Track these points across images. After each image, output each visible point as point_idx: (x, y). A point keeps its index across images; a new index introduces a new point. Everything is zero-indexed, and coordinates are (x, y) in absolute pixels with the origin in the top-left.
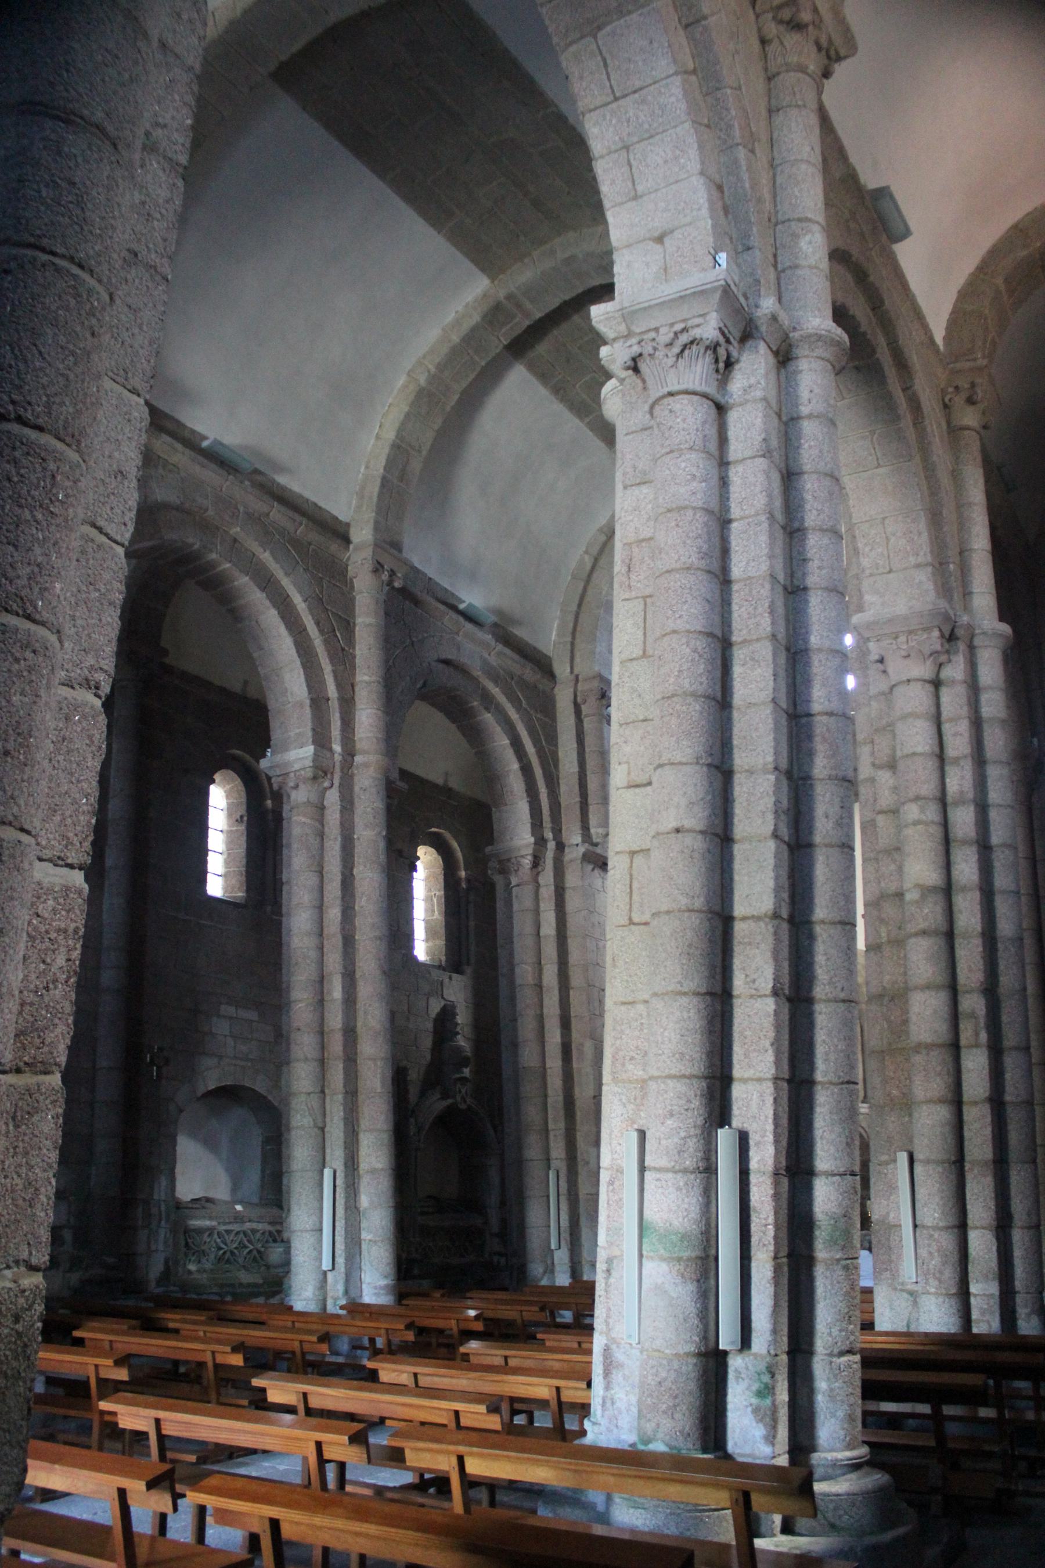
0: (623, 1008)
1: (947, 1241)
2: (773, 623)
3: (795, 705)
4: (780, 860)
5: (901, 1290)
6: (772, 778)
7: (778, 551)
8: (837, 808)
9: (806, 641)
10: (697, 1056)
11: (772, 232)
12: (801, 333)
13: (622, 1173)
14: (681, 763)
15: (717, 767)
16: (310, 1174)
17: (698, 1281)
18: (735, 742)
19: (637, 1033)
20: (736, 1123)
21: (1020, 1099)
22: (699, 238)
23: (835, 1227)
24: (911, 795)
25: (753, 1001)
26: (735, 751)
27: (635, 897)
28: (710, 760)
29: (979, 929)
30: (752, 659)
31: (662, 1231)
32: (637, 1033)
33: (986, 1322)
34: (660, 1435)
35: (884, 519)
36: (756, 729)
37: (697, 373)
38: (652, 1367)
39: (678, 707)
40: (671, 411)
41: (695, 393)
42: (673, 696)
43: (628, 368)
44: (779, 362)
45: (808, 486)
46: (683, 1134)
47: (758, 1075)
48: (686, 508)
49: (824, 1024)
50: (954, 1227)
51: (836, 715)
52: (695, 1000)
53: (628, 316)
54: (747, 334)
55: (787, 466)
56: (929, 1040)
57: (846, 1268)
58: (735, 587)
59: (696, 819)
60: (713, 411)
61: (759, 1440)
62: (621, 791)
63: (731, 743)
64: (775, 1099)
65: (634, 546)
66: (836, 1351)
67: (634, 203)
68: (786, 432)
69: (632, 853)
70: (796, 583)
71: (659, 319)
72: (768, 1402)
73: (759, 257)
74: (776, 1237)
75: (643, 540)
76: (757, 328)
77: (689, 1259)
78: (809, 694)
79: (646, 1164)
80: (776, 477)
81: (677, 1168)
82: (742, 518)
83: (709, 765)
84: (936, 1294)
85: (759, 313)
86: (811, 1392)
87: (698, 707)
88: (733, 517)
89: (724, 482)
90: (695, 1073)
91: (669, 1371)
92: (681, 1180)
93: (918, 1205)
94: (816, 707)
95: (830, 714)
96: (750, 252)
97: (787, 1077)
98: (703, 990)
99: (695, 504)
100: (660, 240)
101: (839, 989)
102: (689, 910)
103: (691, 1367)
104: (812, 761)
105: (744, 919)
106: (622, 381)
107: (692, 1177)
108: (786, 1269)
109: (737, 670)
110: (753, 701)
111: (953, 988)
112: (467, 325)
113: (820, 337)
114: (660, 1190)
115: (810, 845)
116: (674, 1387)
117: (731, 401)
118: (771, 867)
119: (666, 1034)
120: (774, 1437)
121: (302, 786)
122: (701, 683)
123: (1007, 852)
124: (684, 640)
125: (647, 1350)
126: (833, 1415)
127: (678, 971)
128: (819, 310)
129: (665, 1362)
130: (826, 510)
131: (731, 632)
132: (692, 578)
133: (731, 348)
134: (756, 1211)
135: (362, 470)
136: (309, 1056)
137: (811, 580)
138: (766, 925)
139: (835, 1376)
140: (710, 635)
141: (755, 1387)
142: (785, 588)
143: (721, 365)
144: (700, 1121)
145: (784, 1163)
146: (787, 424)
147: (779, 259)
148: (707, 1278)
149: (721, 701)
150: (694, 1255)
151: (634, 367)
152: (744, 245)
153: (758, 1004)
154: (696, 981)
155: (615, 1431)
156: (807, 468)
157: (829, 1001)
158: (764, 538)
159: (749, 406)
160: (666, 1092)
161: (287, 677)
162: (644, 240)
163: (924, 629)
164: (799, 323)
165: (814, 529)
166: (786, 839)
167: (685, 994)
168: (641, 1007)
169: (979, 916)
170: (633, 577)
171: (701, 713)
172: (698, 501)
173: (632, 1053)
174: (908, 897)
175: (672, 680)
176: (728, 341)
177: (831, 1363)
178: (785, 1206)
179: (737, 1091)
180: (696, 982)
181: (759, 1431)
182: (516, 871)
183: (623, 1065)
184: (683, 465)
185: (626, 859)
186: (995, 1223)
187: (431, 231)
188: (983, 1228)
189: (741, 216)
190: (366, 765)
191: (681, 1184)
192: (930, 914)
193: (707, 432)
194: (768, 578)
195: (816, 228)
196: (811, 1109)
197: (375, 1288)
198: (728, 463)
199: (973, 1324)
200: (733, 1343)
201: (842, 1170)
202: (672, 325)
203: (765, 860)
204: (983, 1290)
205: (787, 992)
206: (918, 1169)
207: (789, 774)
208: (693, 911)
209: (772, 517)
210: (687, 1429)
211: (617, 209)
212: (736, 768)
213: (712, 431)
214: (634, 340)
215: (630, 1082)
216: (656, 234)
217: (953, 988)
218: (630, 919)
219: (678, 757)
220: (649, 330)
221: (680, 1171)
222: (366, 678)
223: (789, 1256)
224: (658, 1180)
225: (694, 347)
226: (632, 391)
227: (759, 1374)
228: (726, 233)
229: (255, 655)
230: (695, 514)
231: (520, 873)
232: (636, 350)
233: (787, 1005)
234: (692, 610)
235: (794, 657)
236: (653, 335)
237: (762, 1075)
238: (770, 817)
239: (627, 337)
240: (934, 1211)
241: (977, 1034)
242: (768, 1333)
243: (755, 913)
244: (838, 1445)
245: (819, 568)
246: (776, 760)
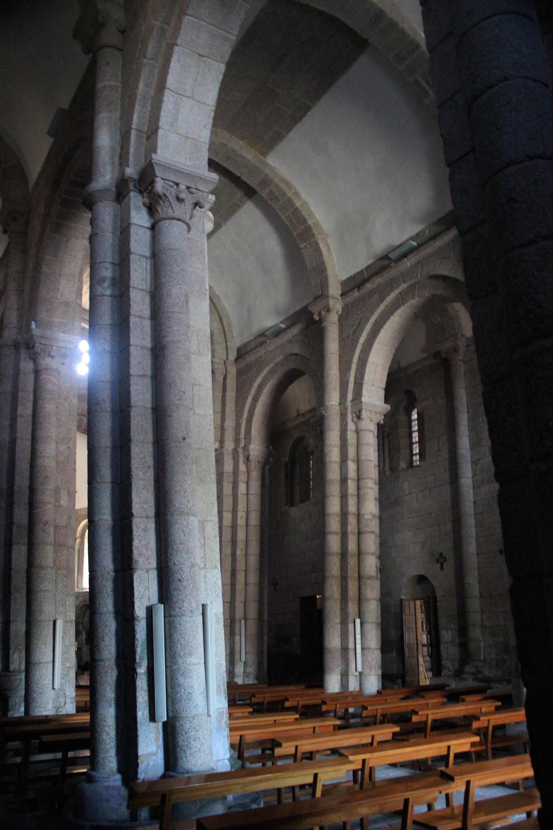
35: (377, 365)
84: (374, 675)
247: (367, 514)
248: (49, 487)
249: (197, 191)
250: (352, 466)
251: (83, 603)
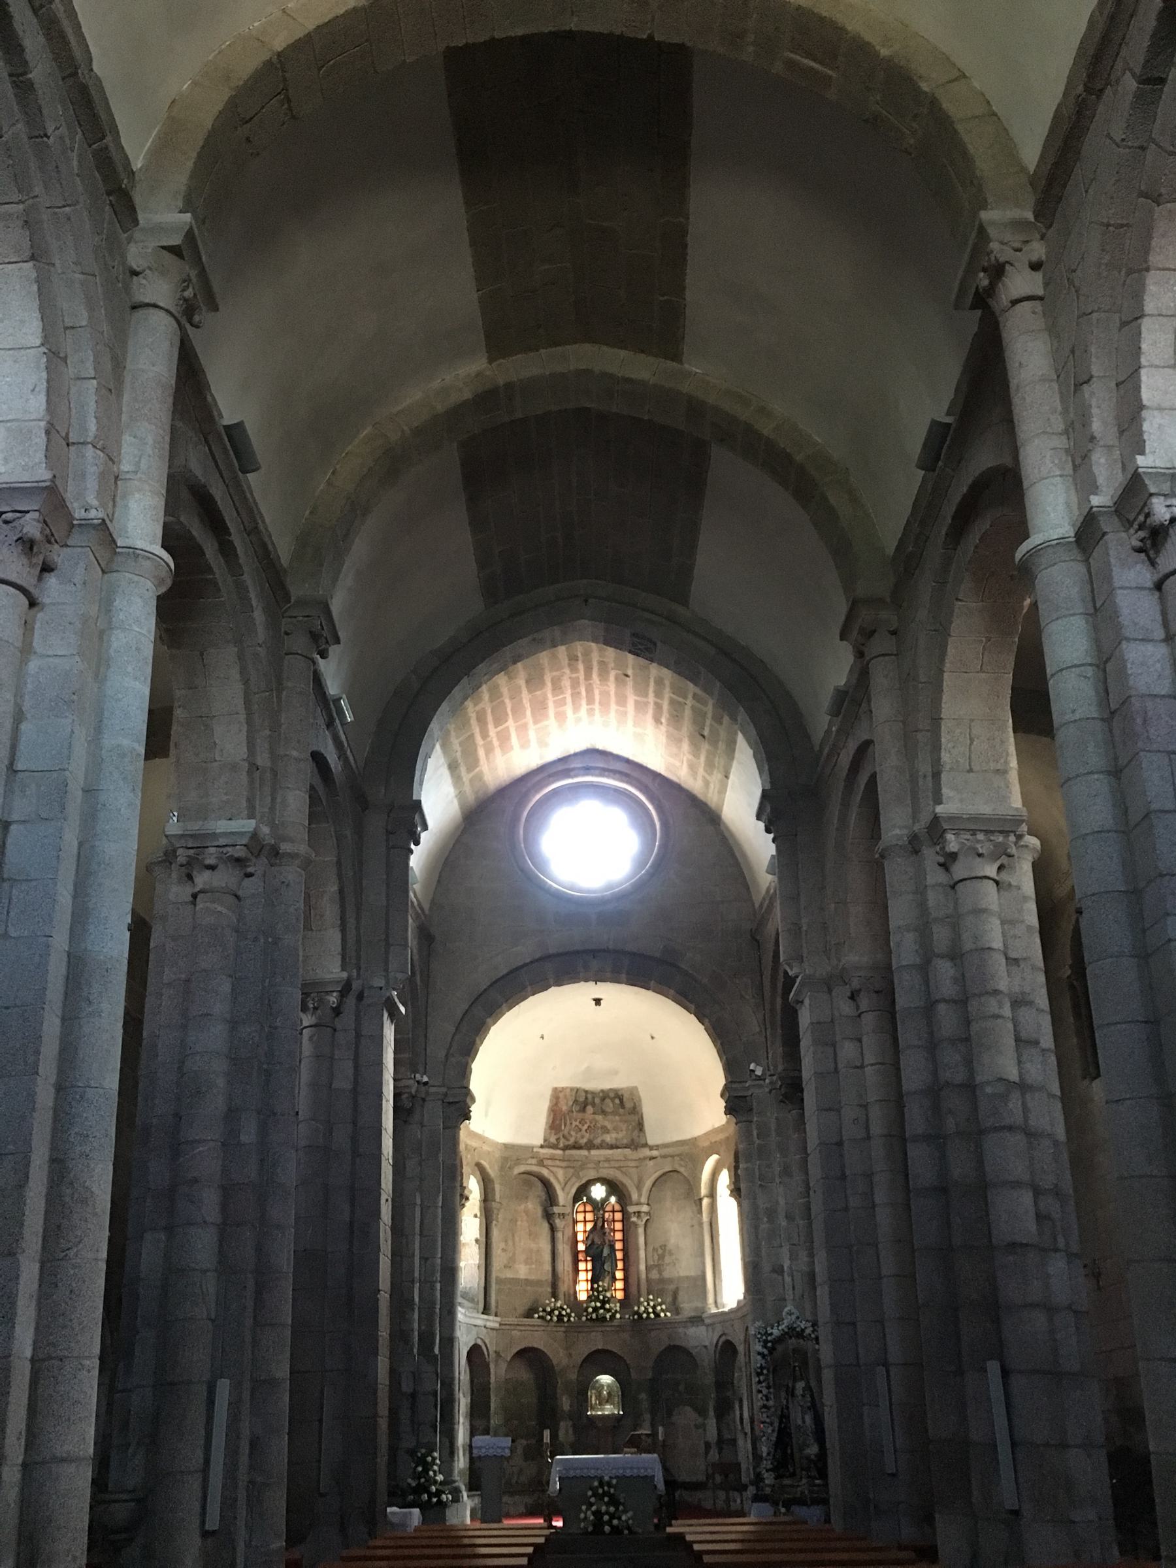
112: (454, 399)
121: (221, 866)
135: (307, 512)
136: (209, 1219)
222: (295, 753)
247: (988, 1083)
249: (18, 515)
250: (944, 970)
251: (723, 1339)
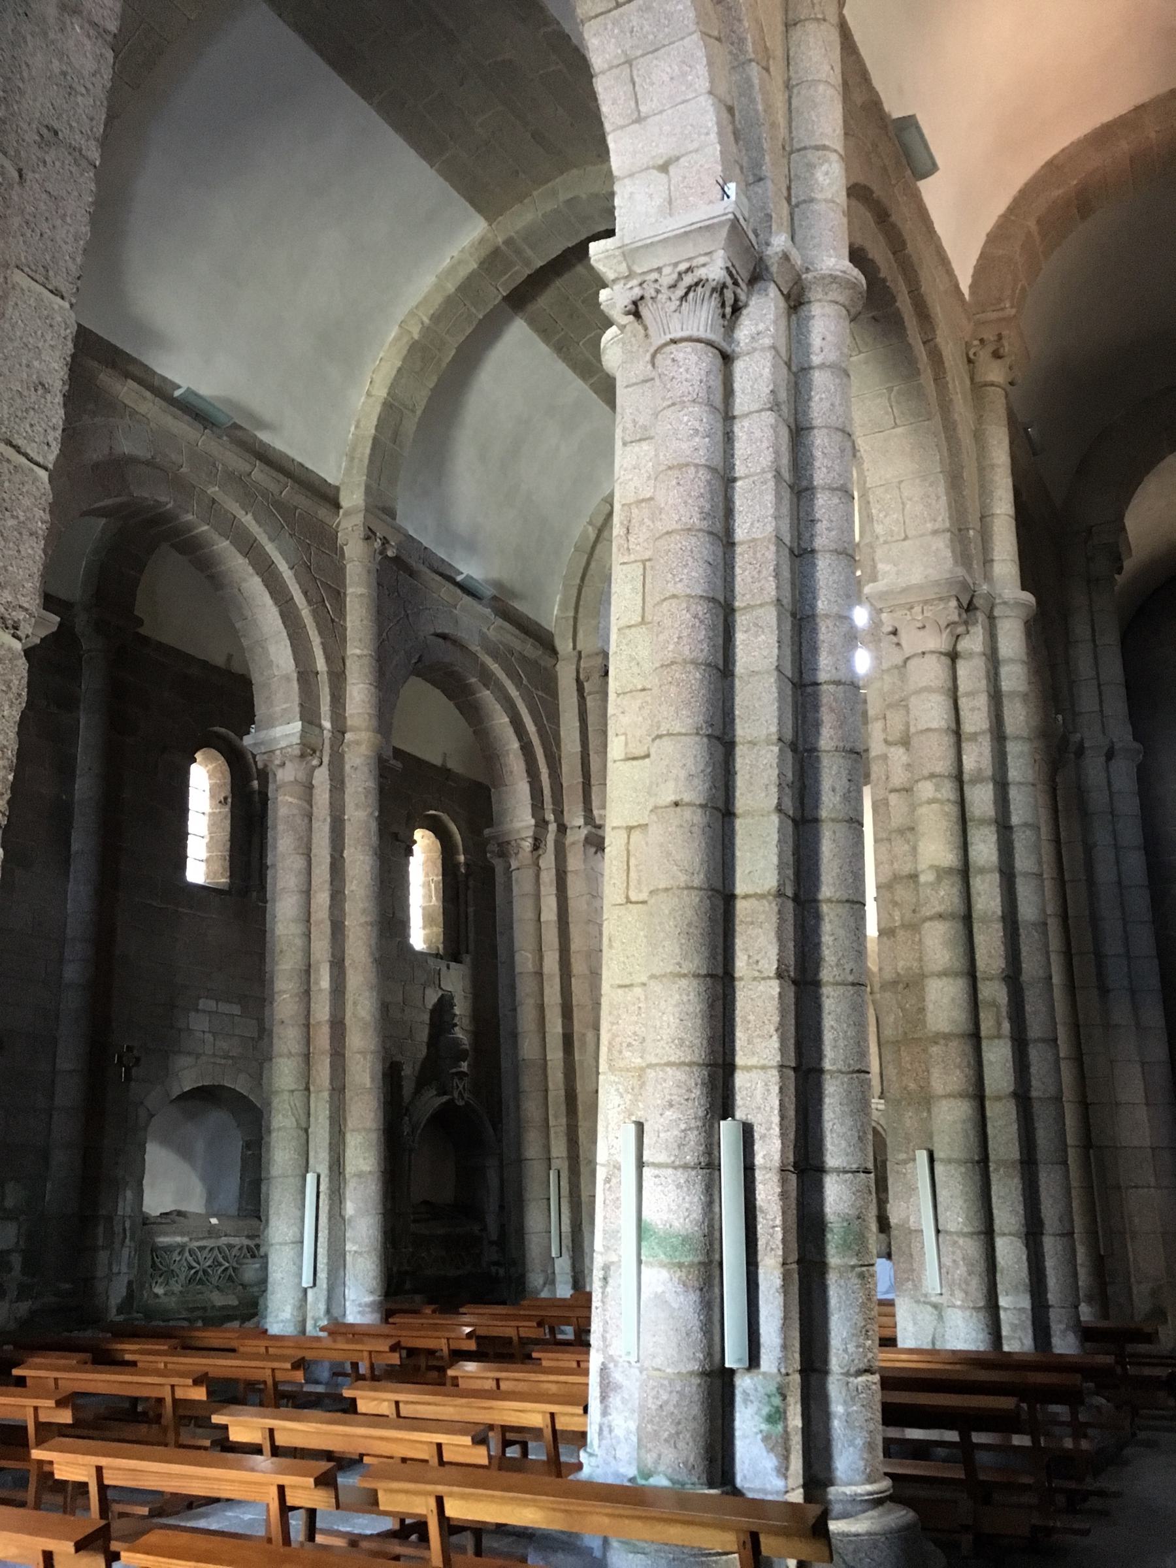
0: (620, 991)
1: (972, 1248)
2: (777, 588)
3: (801, 673)
4: (784, 835)
5: (925, 1303)
6: (776, 749)
7: (785, 510)
8: (845, 780)
9: (813, 607)
10: (697, 1041)
11: (785, 161)
12: (815, 274)
13: (619, 1169)
14: (680, 734)
15: (718, 738)
16: (291, 1180)
17: (701, 1290)
18: (737, 713)
19: (635, 1018)
20: (739, 1114)
21: (1048, 1095)
22: (706, 166)
23: (847, 1230)
24: (926, 773)
25: (755, 983)
26: (737, 721)
27: (633, 874)
28: (710, 731)
29: (1000, 913)
30: (756, 625)
31: (661, 1233)
32: (635, 1018)
33: (1017, 1340)
34: (662, 1468)
35: (901, 482)
36: (759, 699)
37: (701, 319)
38: (653, 1389)
39: (677, 675)
40: (673, 360)
41: (699, 340)
42: (673, 663)
43: (628, 313)
44: (790, 307)
45: (818, 442)
46: (683, 1126)
47: (762, 1062)
48: (687, 465)
49: (833, 1008)
50: (979, 1233)
51: (844, 684)
52: (695, 982)
53: (629, 254)
54: (757, 276)
55: (796, 420)
56: (947, 1030)
57: (861, 1276)
58: (739, 550)
59: (695, 793)
60: (719, 360)
61: (769, 1470)
62: (618, 763)
63: (733, 712)
64: (781, 1088)
65: (633, 507)
66: (853, 1370)
67: (637, 126)
68: (796, 384)
69: (630, 829)
70: (804, 546)
71: (663, 258)
72: (780, 1427)
73: (773, 188)
74: (784, 1241)
75: (643, 500)
76: (767, 269)
77: (691, 1265)
78: (816, 662)
79: (645, 1159)
80: (784, 433)
81: (677, 1163)
82: (747, 477)
83: (708, 736)
84: (959, 1307)
85: (770, 251)
86: (826, 1416)
87: (698, 675)
88: (737, 475)
89: (729, 438)
90: (695, 1060)
91: (671, 1392)
92: (681, 1176)
93: (940, 1209)
94: (822, 676)
95: (838, 683)
96: (761, 183)
97: (793, 1065)
98: (703, 972)
99: (697, 461)
100: (664, 168)
101: (848, 971)
102: (688, 888)
103: (694, 1388)
104: (819, 733)
105: (746, 897)
106: (622, 328)
107: (693, 1173)
108: (796, 1276)
109: (740, 637)
110: (756, 669)
111: (971, 974)
112: (463, 273)
113: (834, 279)
114: (660, 1188)
115: (817, 820)
116: (676, 1412)
117: (738, 349)
118: (775, 842)
119: (665, 1018)
120: (787, 1469)
122: (702, 651)
123: (1028, 832)
124: (684, 605)
125: (647, 1369)
126: (851, 1443)
127: (677, 951)
128: (834, 249)
129: (666, 1382)
130: (837, 467)
131: (734, 598)
132: (693, 540)
133: (739, 291)
134: (762, 1212)
135: (353, 429)
136: (293, 1051)
137: (820, 542)
138: (770, 903)
139: (853, 1399)
140: (713, 600)
141: (766, 1410)
142: (791, 551)
143: (728, 310)
144: (701, 1113)
145: (792, 1159)
146: (796, 375)
147: (793, 192)
148: (711, 1286)
149: (722, 670)
150: (696, 1260)
151: (635, 312)
152: (755, 175)
153: (762, 987)
154: (696, 962)
155: (613, 1462)
156: (817, 422)
157: (837, 984)
158: (769, 498)
159: (756, 354)
160: (665, 1081)
161: (272, 649)
162: (648, 168)
163: (941, 599)
164: (812, 264)
165: (823, 488)
166: (791, 813)
167: (685, 976)
168: (638, 991)
169: (999, 899)
170: (632, 539)
171: (702, 681)
172: (701, 458)
173: (629, 1040)
174: (923, 879)
175: (671, 647)
176: (736, 283)
177: (848, 1383)
178: (794, 1206)
179: (740, 1079)
180: (696, 963)
181: (769, 1462)
182: (517, 854)
183: (620, 1052)
184: (686, 419)
185: (623, 834)
186: (1023, 1230)
187: (424, 164)
188: (1013, 1235)
189: (752, 143)
190: (358, 743)
191: (682, 1181)
192: (945, 897)
193: (711, 383)
194: (774, 539)
195: (834, 157)
196: (820, 1101)
197: (360, 1305)
198: (734, 418)
199: (1004, 1342)
200: (740, 1360)
201: (854, 1166)
202: (676, 265)
203: (769, 834)
204: (1014, 1304)
205: (792, 974)
206: (939, 1168)
207: (794, 747)
208: (692, 888)
209: (778, 475)
210: (692, 1459)
211: (619, 132)
212: (738, 739)
213: (717, 383)
214: (635, 282)
215: (628, 1070)
216: (661, 162)
217: (971, 974)
218: (627, 897)
219: (677, 728)
220: (651, 271)
221: (680, 1166)
222: (358, 652)
223: (799, 1262)
224: (657, 1176)
225: (699, 289)
226: (633, 339)
227: (769, 1396)
228: (736, 162)
229: (238, 625)
230: (697, 472)
231: (520, 856)
232: (637, 292)
233: (793, 988)
234: (693, 574)
235: (800, 623)
236: (655, 275)
237: (766, 1062)
238: (774, 790)
239: (627, 278)
240: (957, 1217)
241: (999, 1024)
242: (779, 1349)
243: (759, 892)
244: (857, 1478)
245: (827, 529)
246: (779, 731)
248: (284, 967)
